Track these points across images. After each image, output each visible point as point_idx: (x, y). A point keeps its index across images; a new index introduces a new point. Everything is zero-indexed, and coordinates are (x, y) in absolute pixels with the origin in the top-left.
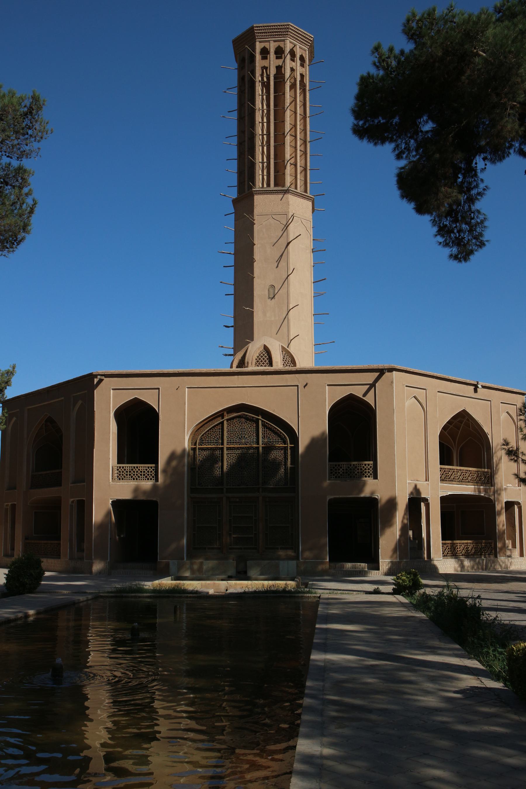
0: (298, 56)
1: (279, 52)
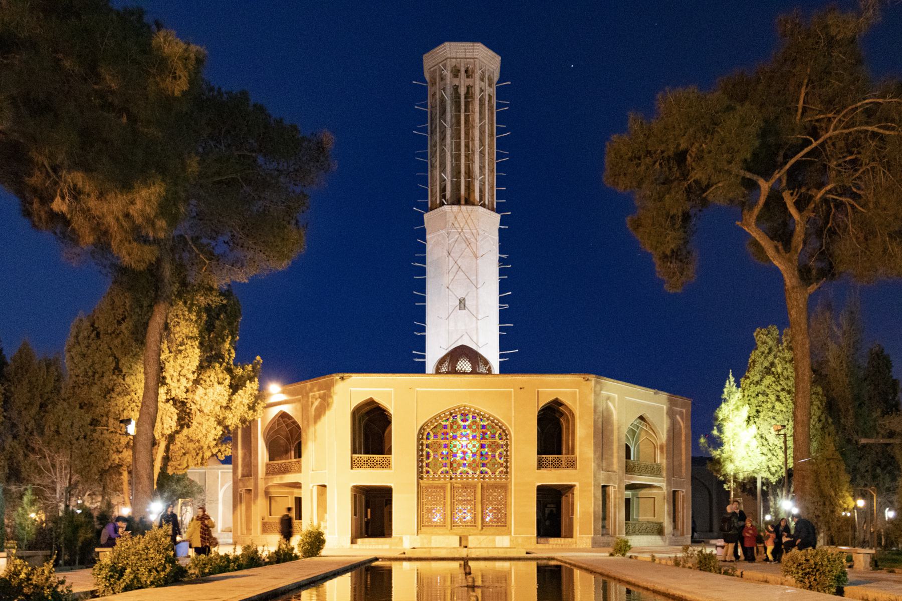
0: (487, 76)
1: (469, 73)
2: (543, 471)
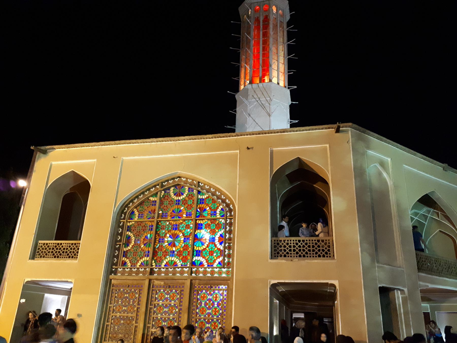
2: (281, 261)
